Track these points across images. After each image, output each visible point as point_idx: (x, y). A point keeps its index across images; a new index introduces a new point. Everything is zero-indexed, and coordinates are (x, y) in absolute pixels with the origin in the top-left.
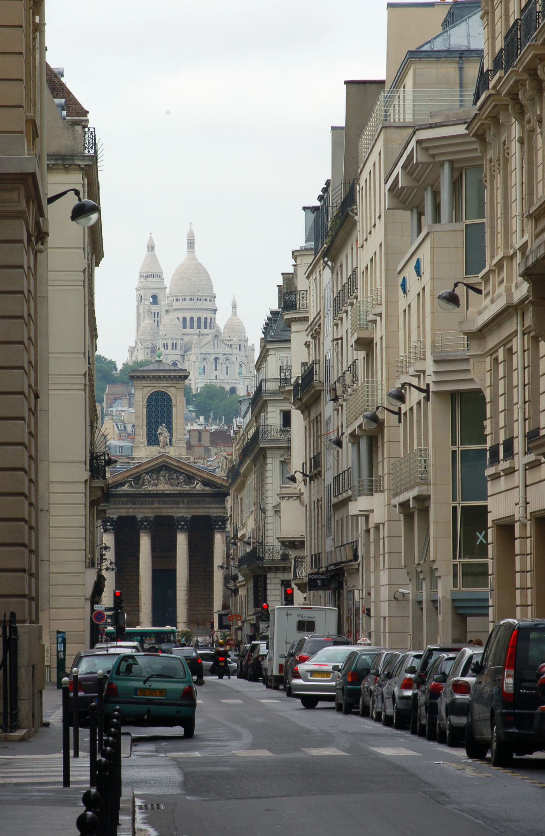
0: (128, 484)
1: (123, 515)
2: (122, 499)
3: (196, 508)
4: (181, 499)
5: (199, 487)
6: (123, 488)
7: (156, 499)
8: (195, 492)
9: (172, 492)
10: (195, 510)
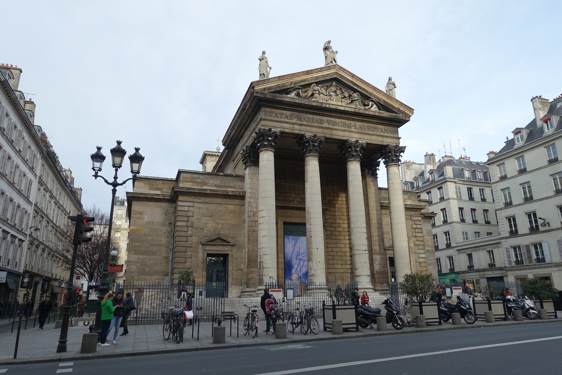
0: (295, 92)
1: (287, 131)
2: (285, 112)
3: (370, 134)
4: (353, 123)
5: (374, 108)
6: (289, 96)
7: (325, 118)
8: (371, 113)
9: (346, 109)
10: (369, 137)
